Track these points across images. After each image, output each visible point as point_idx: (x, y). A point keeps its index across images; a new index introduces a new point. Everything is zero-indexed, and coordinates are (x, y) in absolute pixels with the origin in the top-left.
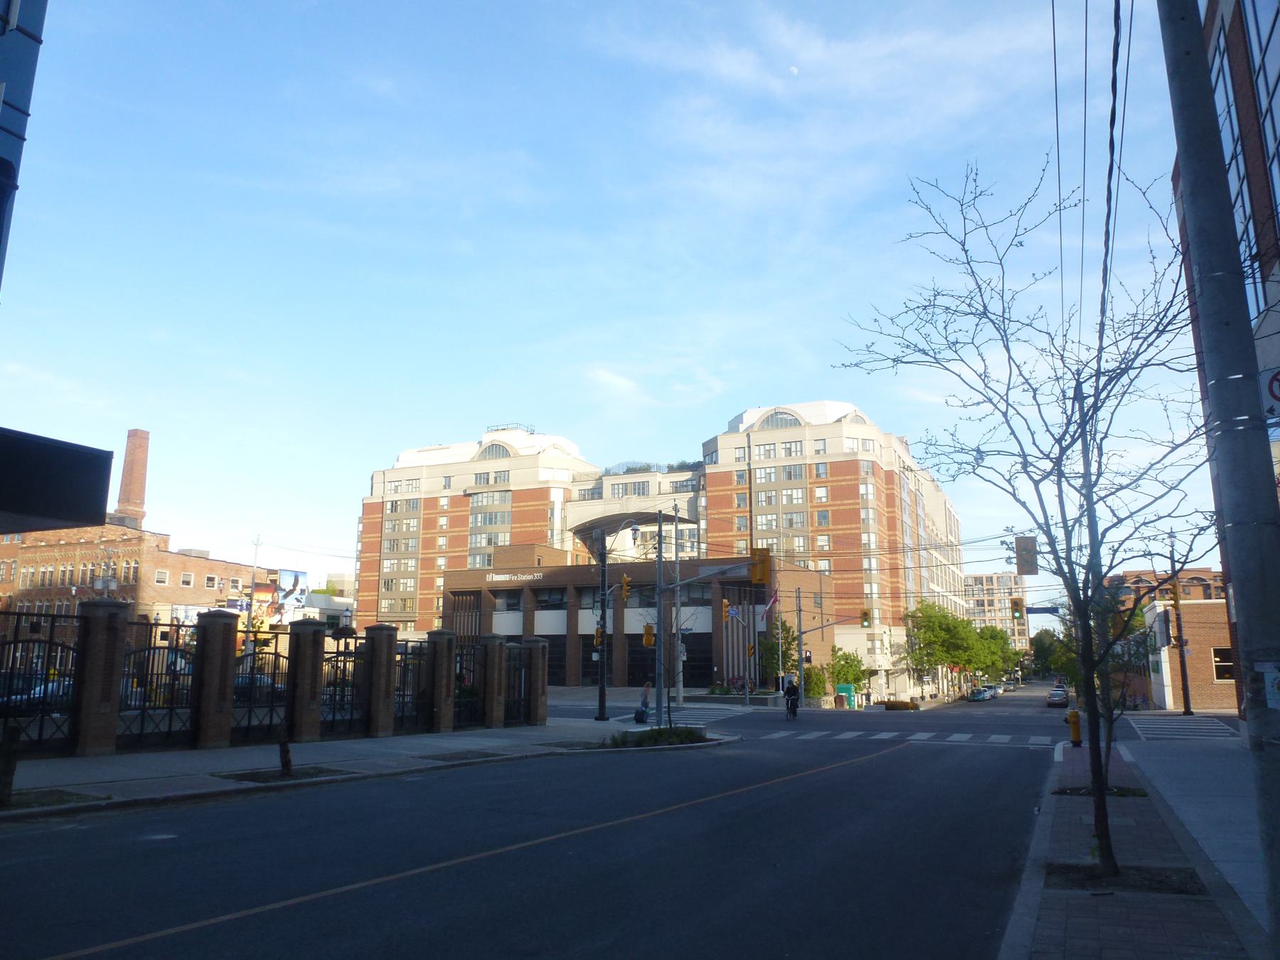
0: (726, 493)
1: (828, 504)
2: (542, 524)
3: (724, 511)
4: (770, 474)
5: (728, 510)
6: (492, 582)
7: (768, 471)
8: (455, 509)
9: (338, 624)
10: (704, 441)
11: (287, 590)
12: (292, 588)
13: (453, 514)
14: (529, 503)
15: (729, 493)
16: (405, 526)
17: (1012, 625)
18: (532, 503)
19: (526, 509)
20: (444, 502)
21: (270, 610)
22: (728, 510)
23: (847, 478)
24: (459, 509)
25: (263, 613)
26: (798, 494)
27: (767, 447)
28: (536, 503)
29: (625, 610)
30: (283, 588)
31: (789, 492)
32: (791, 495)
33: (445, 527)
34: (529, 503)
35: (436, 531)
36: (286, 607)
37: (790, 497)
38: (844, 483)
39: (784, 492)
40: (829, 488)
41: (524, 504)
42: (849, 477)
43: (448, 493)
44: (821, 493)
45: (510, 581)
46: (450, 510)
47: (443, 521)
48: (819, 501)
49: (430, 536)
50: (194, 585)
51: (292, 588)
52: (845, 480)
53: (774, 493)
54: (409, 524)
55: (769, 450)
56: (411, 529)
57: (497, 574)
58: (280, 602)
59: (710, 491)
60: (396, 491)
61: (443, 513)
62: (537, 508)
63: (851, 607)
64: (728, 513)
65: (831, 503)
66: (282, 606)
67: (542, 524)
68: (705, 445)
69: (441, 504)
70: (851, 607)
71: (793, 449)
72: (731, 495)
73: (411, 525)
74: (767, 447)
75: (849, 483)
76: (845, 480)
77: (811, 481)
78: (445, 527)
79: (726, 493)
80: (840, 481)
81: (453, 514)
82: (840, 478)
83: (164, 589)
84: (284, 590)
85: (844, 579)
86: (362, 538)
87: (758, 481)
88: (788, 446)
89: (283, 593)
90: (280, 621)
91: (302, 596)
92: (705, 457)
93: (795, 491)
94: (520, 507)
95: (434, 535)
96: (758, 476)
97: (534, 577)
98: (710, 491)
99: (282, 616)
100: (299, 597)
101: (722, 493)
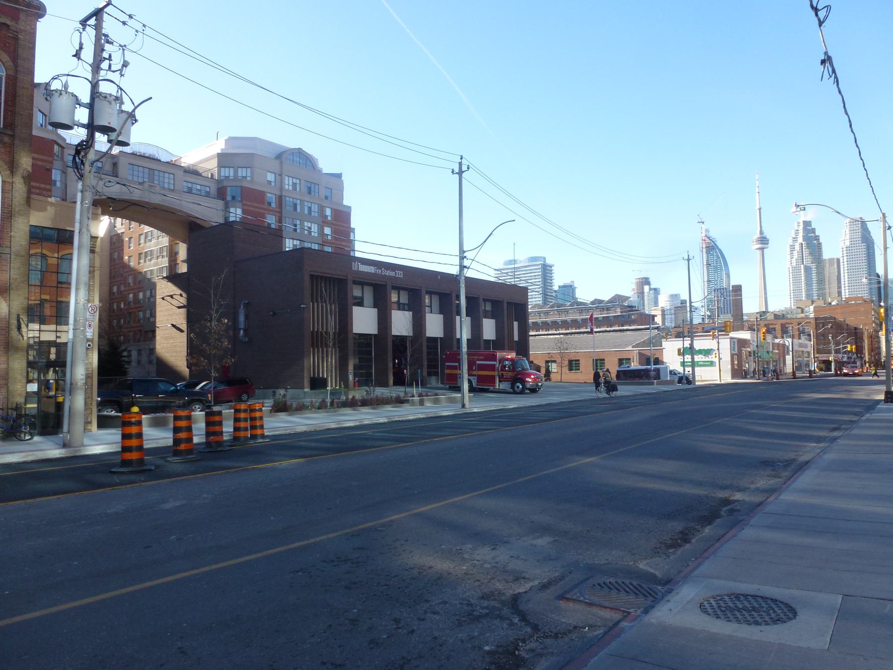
0: (260, 210)
1: (331, 241)
2: (43, 186)
6: (358, 272)
15: (262, 211)
26: (315, 228)
27: (295, 181)
39: (306, 224)
40: (333, 229)
44: (327, 231)
45: (375, 274)
48: (326, 238)
53: (298, 222)
55: (296, 184)
59: (246, 205)
65: (333, 241)
67: (43, 186)
71: (312, 189)
72: (264, 213)
74: (295, 181)
79: (260, 210)
87: (288, 208)
88: (309, 185)
98: (246, 205)
101: (256, 210)
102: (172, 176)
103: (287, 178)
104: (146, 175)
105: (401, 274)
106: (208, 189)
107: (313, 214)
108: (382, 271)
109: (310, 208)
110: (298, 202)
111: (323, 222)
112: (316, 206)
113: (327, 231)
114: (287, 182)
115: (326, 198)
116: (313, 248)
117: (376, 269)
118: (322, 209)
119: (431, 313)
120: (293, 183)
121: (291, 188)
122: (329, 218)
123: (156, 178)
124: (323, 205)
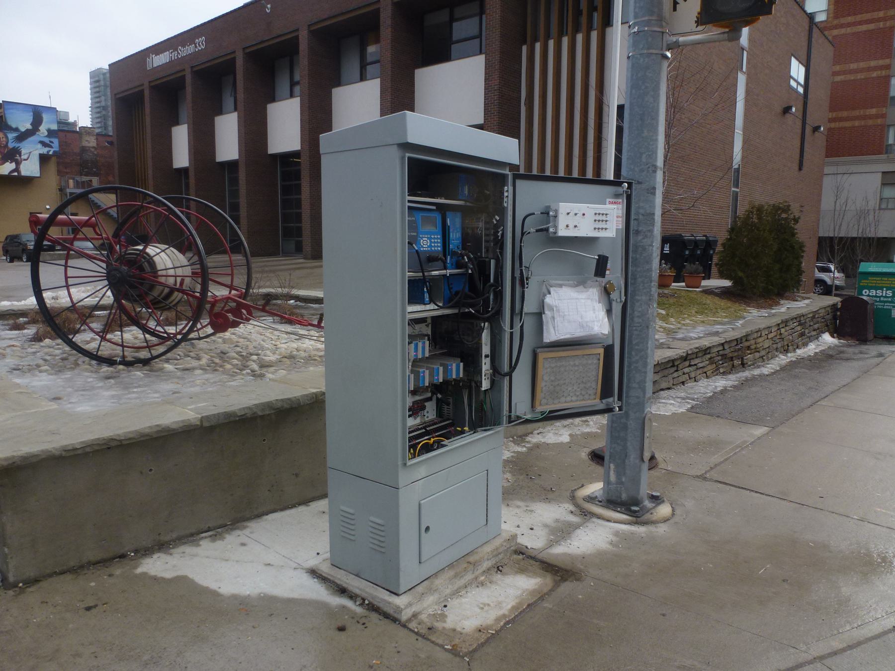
11: (23, 129)
12: (29, 126)
30: (14, 126)
36: (23, 152)
51: (29, 127)
57: (156, 55)
58: (11, 145)
63: (857, 123)
70: (857, 123)
84: (17, 130)
85: (851, 72)
89: (15, 135)
90: (17, 170)
91: (52, 140)
97: (196, 47)
99: (18, 163)
105: (203, 44)
108: (178, 53)
117: (171, 52)
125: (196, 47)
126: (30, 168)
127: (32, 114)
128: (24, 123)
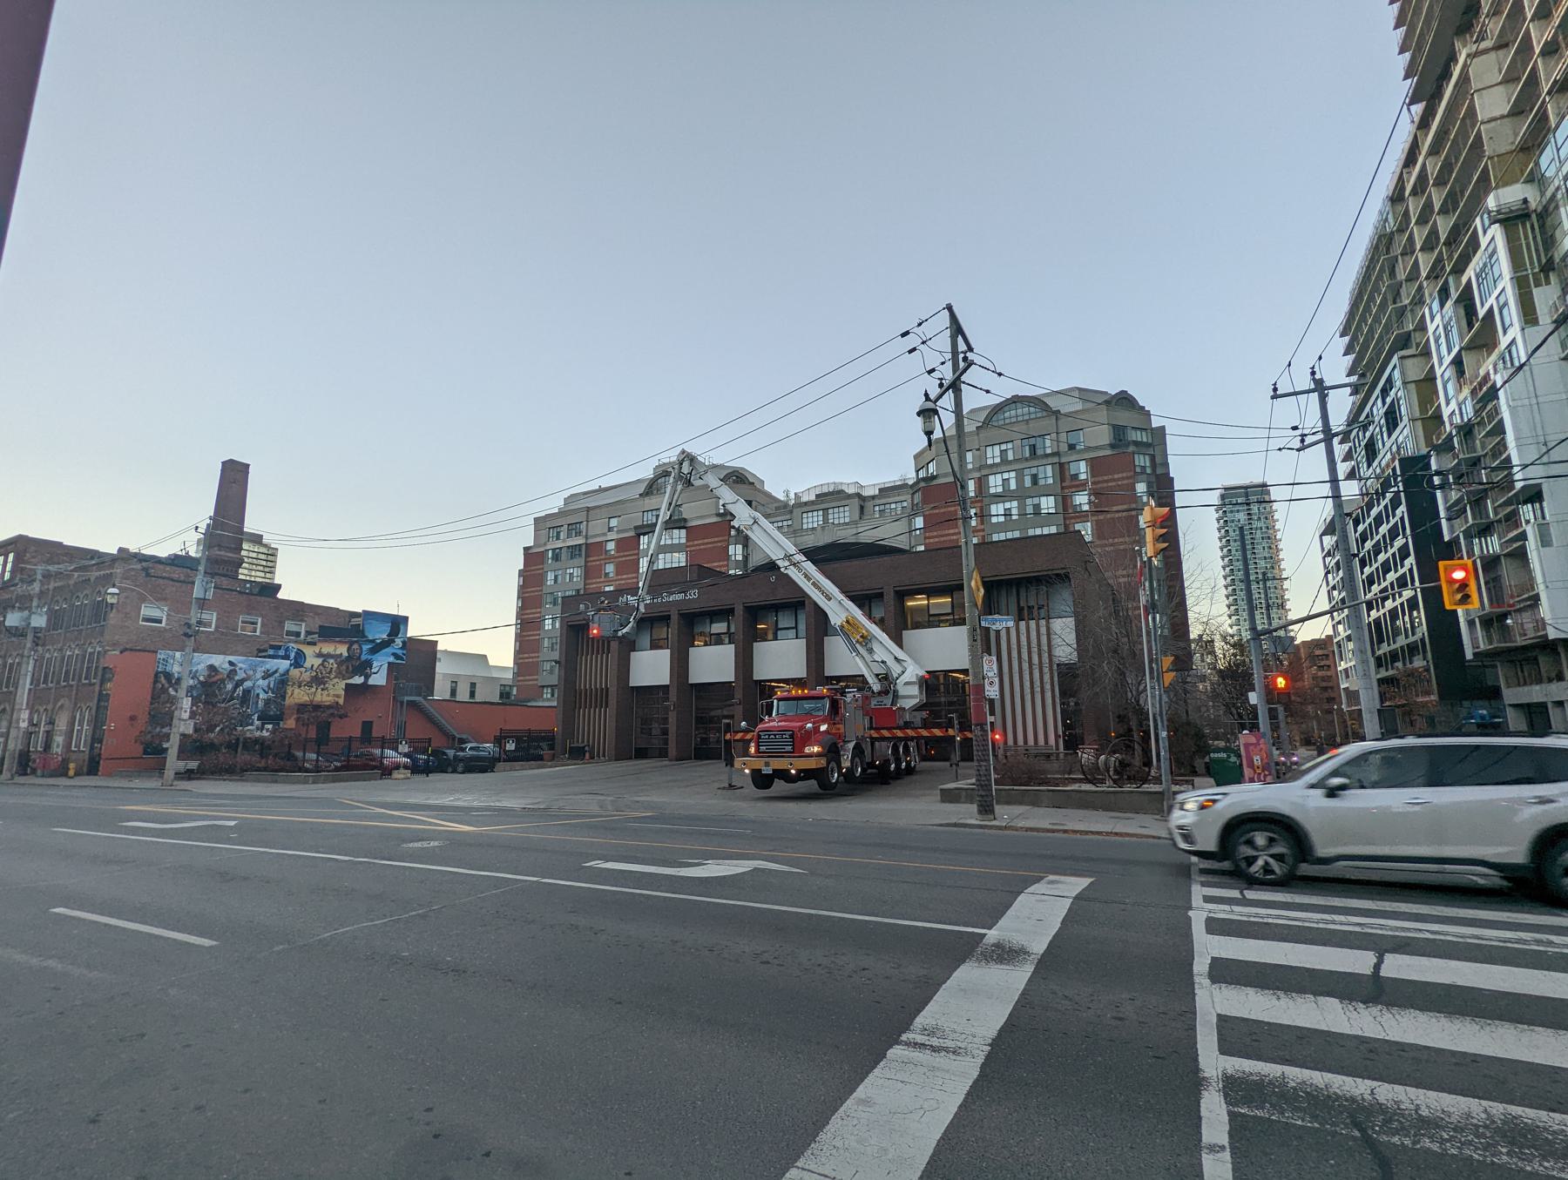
3: (947, 532)
4: (1008, 479)
5: (952, 531)
7: (1006, 476)
8: (622, 554)
9: (322, 664)
10: (915, 453)
11: (378, 641)
12: (385, 636)
13: (620, 559)
14: (706, 541)
16: (568, 576)
17: (1425, 663)
18: (710, 540)
19: (702, 547)
20: (611, 546)
21: (344, 667)
22: (952, 531)
23: (1116, 476)
24: (626, 553)
25: (330, 672)
26: (1048, 504)
28: (713, 540)
29: (825, 638)
31: (1036, 501)
32: (1039, 504)
33: (611, 575)
34: (706, 541)
35: (602, 580)
37: (1037, 507)
38: (1110, 484)
39: (1029, 501)
41: (700, 542)
42: (1120, 475)
43: (612, 536)
44: (1082, 500)
46: (619, 554)
47: (610, 568)
48: (1078, 510)
49: (594, 586)
50: (217, 627)
51: (385, 636)
52: (1114, 480)
54: (573, 573)
56: (575, 579)
60: (558, 538)
61: (609, 559)
62: (715, 545)
64: (953, 534)
66: (369, 664)
68: (916, 457)
69: (608, 549)
71: (1038, 446)
72: (956, 511)
73: (575, 574)
74: (1004, 447)
75: (1120, 483)
76: (1114, 480)
77: (1064, 484)
78: (611, 575)
80: (1107, 481)
81: (620, 559)
82: (1106, 478)
83: (160, 631)
86: (523, 593)
88: (1032, 441)
92: (917, 471)
93: (1043, 499)
94: (697, 545)
95: (601, 585)
96: (992, 483)
97: (686, 595)
100: (400, 652)
102: (847, 508)
103: (989, 449)
104: (821, 518)
106: (905, 504)
107: (1042, 482)
109: (1035, 478)
110: (1013, 474)
111: (1063, 488)
112: (1049, 468)
113: (1082, 500)
114: (989, 454)
115: (1072, 447)
116: (1044, 533)
118: (1062, 469)
119: (797, 638)
120: (1001, 451)
121: (998, 460)
122: (1083, 477)
123: (831, 516)
124: (1063, 460)
125: (686, 595)
126: (379, 678)
127: (390, 624)
128: (380, 633)
